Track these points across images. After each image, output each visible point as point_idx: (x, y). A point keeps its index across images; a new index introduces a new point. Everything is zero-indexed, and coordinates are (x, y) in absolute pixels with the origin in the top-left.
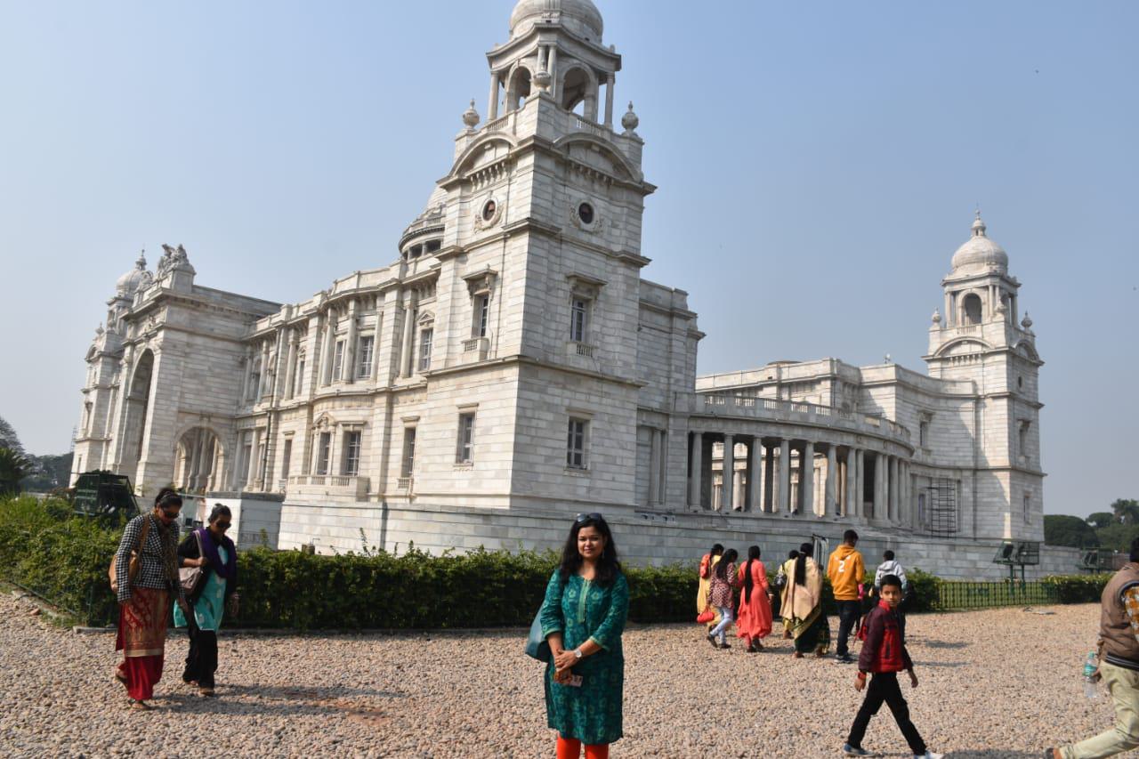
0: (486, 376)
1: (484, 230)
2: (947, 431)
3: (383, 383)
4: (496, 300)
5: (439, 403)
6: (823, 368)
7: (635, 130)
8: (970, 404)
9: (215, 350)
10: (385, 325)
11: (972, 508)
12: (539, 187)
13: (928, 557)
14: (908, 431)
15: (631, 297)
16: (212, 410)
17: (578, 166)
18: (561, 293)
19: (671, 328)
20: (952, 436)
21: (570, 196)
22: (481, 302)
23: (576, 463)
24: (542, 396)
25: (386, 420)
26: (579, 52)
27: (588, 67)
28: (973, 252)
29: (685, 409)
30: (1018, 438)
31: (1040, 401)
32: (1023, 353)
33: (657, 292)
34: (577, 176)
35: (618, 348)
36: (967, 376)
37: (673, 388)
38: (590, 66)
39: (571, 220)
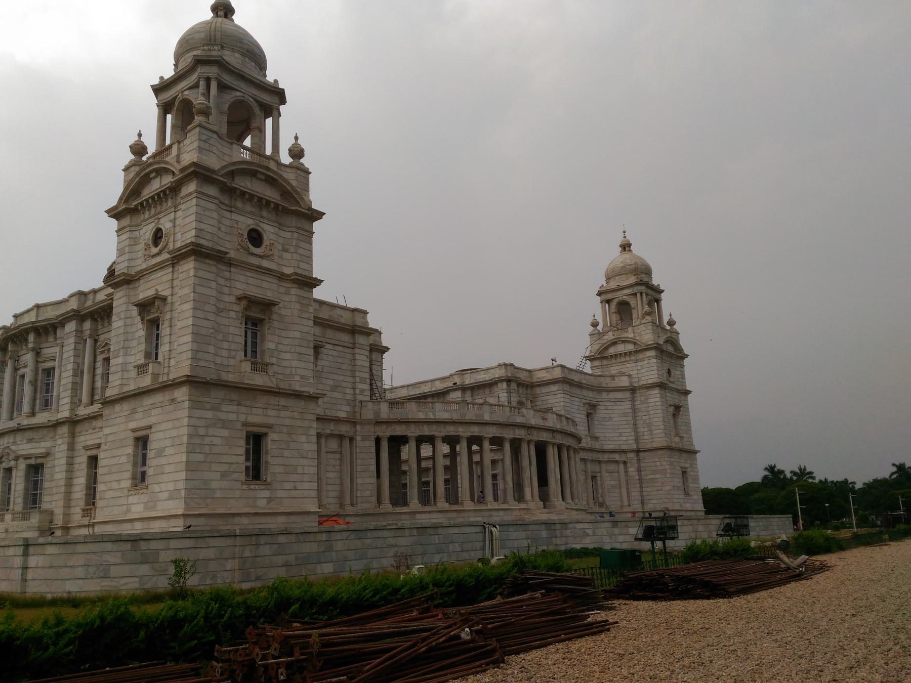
0: (158, 398)
1: (153, 256)
2: (610, 419)
3: (64, 414)
4: (167, 324)
5: (115, 429)
7: (302, 161)
10: (65, 355)
11: (638, 485)
12: (202, 213)
13: (594, 535)
14: (573, 421)
15: (304, 315)
17: (243, 194)
19: (354, 344)
20: (615, 423)
21: (237, 222)
22: (153, 325)
25: (68, 450)
26: (242, 85)
28: (622, 265)
29: (370, 416)
30: (672, 422)
31: (688, 388)
32: (670, 348)
33: (339, 312)
34: (244, 203)
35: (295, 364)
36: (623, 370)
37: (359, 398)
39: (239, 244)
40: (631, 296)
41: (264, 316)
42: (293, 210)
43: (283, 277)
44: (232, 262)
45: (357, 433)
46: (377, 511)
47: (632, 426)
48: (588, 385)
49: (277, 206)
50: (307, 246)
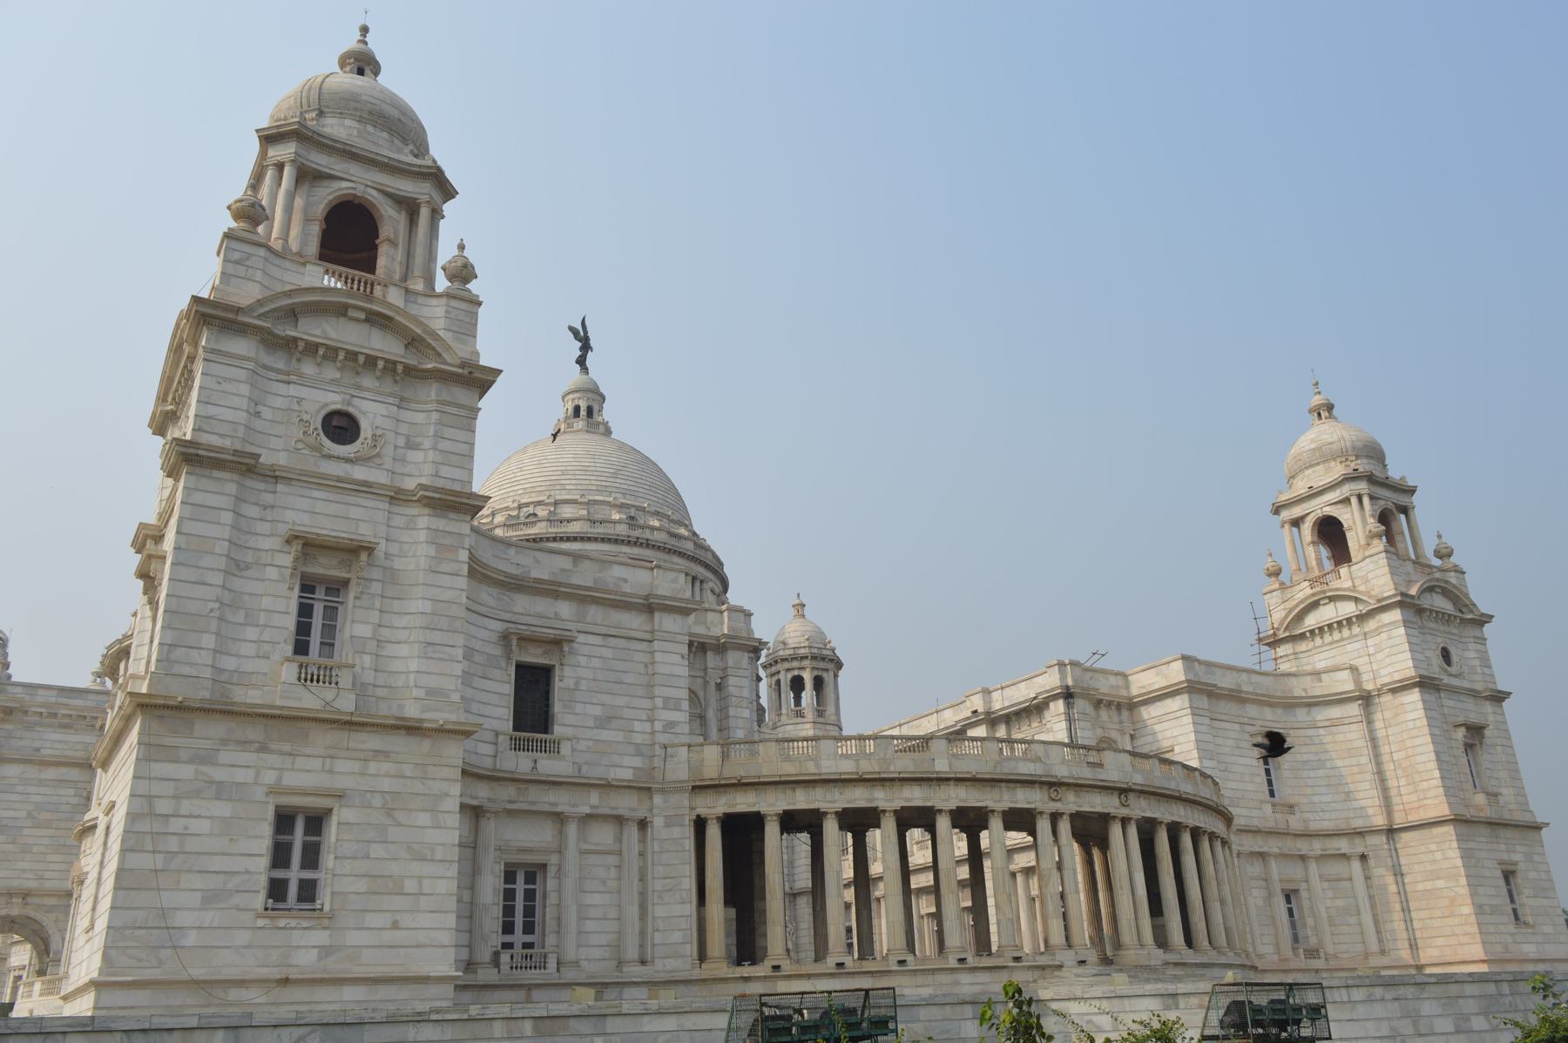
6: (1050, 681)
8: (1354, 709)
9: (41, 783)
12: (218, 387)
15: (445, 567)
16: (32, 884)
18: (272, 573)
21: (300, 401)
23: (301, 899)
24: (204, 768)
26: (355, 170)
27: (374, 193)
28: (1313, 446)
30: (1464, 760)
32: (1440, 603)
34: (319, 365)
37: (662, 738)
38: (380, 191)
40: (1339, 506)
41: (349, 572)
42: (428, 371)
43: (400, 497)
44: (277, 473)
45: (655, 811)
46: (697, 973)
47: (1369, 776)
48: (1257, 695)
49: (391, 366)
50: (461, 435)
